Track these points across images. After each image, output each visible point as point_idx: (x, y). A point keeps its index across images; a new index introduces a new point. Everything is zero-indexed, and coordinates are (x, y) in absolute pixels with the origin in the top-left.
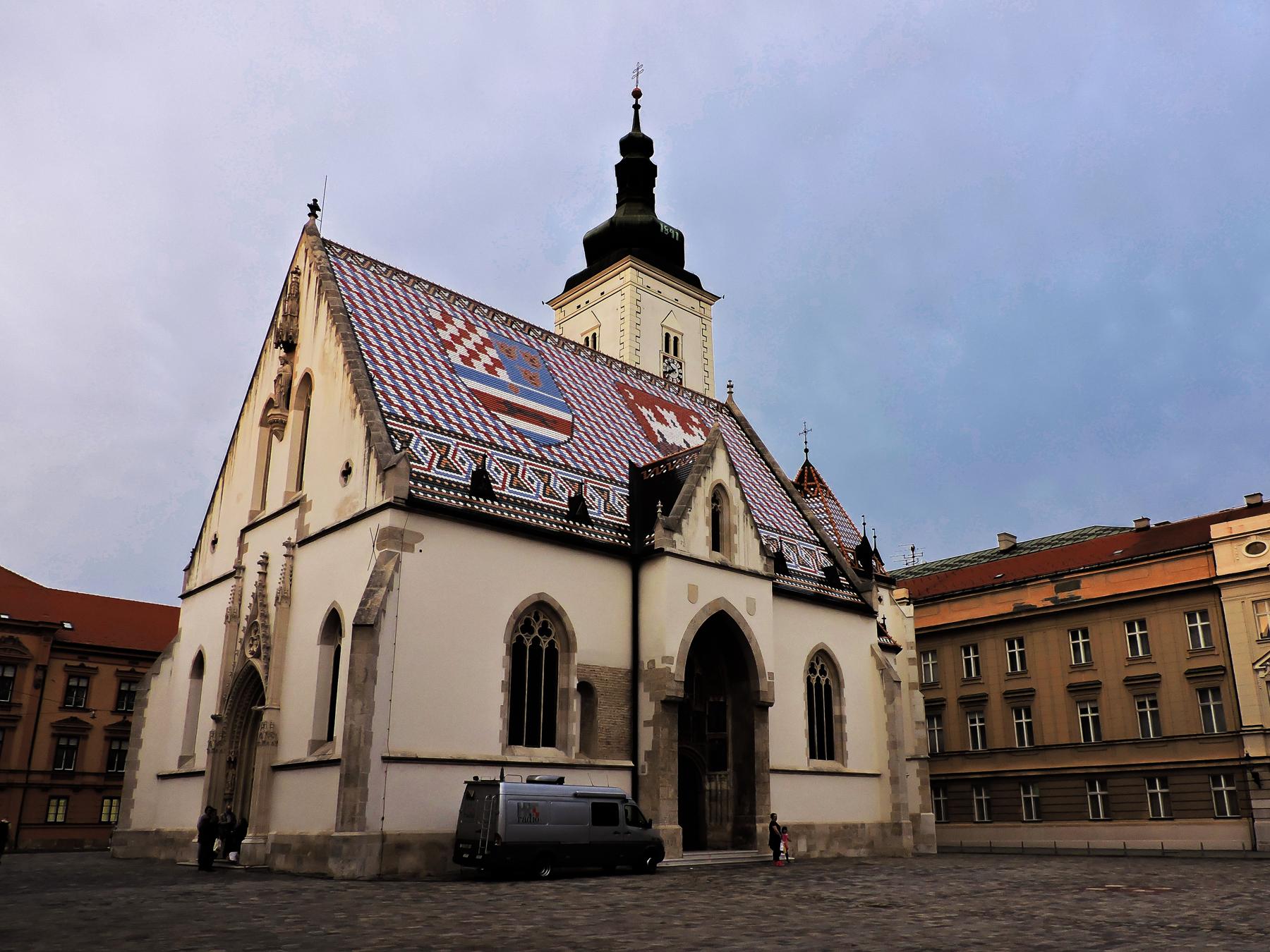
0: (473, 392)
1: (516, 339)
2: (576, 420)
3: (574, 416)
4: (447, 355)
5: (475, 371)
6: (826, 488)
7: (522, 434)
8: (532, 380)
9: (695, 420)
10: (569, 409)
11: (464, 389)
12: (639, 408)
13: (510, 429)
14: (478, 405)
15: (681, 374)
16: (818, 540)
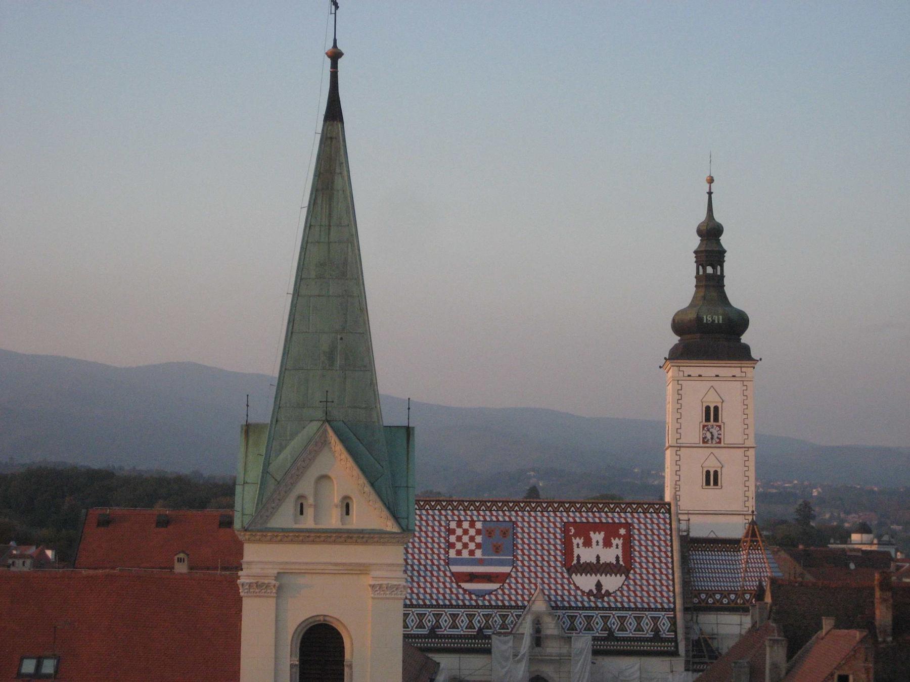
0: (453, 574)
1: (501, 519)
2: (514, 570)
3: (514, 567)
4: (447, 553)
5: (462, 559)
6: (757, 541)
7: (470, 593)
8: (497, 550)
9: (622, 531)
10: (513, 563)
11: (448, 574)
12: (574, 540)
13: (465, 590)
14: (452, 582)
15: (721, 434)
16: (672, 606)
